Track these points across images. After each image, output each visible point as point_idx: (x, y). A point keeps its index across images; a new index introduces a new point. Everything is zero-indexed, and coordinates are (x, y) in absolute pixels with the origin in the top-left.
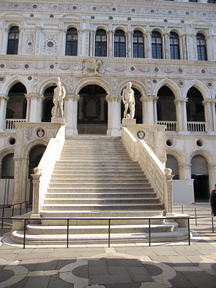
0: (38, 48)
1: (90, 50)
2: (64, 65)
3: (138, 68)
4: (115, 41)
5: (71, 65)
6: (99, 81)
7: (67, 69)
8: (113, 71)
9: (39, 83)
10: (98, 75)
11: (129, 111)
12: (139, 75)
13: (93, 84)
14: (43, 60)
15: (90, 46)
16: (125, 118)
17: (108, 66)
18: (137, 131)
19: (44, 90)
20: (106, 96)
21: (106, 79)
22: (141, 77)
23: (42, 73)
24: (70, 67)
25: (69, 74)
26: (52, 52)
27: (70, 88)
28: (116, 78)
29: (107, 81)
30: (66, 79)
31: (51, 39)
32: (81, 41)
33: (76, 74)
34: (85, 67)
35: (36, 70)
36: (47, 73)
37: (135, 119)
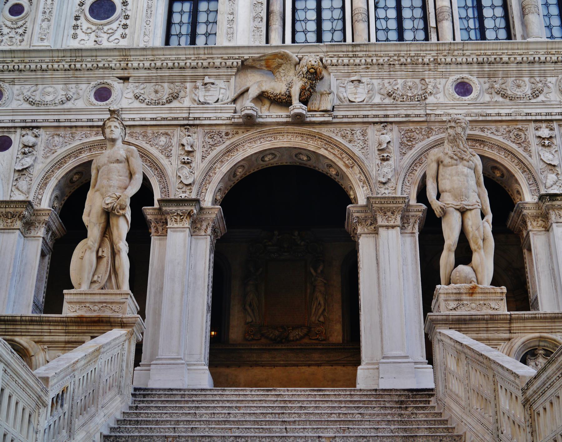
0: (49, 21)
1: (272, 22)
2: (158, 87)
3: (487, 86)
5: (188, 85)
6: (311, 145)
8: (377, 100)
9: (40, 159)
10: (308, 119)
11: (464, 254)
12: (496, 111)
13: (286, 161)
14: (67, 66)
15: (271, 8)
16: (449, 283)
17: (352, 81)
18: (516, 347)
19: (63, 193)
21: (344, 137)
22: (504, 118)
23: (58, 121)
24: (182, 94)
25: (176, 119)
26: (106, 36)
27: (180, 177)
28: (391, 130)
29: (350, 141)
30: (162, 143)
33: (209, 119)
34: (247, 90)
35: (34, 107)
36: (77, 120)
37: (504, 289)
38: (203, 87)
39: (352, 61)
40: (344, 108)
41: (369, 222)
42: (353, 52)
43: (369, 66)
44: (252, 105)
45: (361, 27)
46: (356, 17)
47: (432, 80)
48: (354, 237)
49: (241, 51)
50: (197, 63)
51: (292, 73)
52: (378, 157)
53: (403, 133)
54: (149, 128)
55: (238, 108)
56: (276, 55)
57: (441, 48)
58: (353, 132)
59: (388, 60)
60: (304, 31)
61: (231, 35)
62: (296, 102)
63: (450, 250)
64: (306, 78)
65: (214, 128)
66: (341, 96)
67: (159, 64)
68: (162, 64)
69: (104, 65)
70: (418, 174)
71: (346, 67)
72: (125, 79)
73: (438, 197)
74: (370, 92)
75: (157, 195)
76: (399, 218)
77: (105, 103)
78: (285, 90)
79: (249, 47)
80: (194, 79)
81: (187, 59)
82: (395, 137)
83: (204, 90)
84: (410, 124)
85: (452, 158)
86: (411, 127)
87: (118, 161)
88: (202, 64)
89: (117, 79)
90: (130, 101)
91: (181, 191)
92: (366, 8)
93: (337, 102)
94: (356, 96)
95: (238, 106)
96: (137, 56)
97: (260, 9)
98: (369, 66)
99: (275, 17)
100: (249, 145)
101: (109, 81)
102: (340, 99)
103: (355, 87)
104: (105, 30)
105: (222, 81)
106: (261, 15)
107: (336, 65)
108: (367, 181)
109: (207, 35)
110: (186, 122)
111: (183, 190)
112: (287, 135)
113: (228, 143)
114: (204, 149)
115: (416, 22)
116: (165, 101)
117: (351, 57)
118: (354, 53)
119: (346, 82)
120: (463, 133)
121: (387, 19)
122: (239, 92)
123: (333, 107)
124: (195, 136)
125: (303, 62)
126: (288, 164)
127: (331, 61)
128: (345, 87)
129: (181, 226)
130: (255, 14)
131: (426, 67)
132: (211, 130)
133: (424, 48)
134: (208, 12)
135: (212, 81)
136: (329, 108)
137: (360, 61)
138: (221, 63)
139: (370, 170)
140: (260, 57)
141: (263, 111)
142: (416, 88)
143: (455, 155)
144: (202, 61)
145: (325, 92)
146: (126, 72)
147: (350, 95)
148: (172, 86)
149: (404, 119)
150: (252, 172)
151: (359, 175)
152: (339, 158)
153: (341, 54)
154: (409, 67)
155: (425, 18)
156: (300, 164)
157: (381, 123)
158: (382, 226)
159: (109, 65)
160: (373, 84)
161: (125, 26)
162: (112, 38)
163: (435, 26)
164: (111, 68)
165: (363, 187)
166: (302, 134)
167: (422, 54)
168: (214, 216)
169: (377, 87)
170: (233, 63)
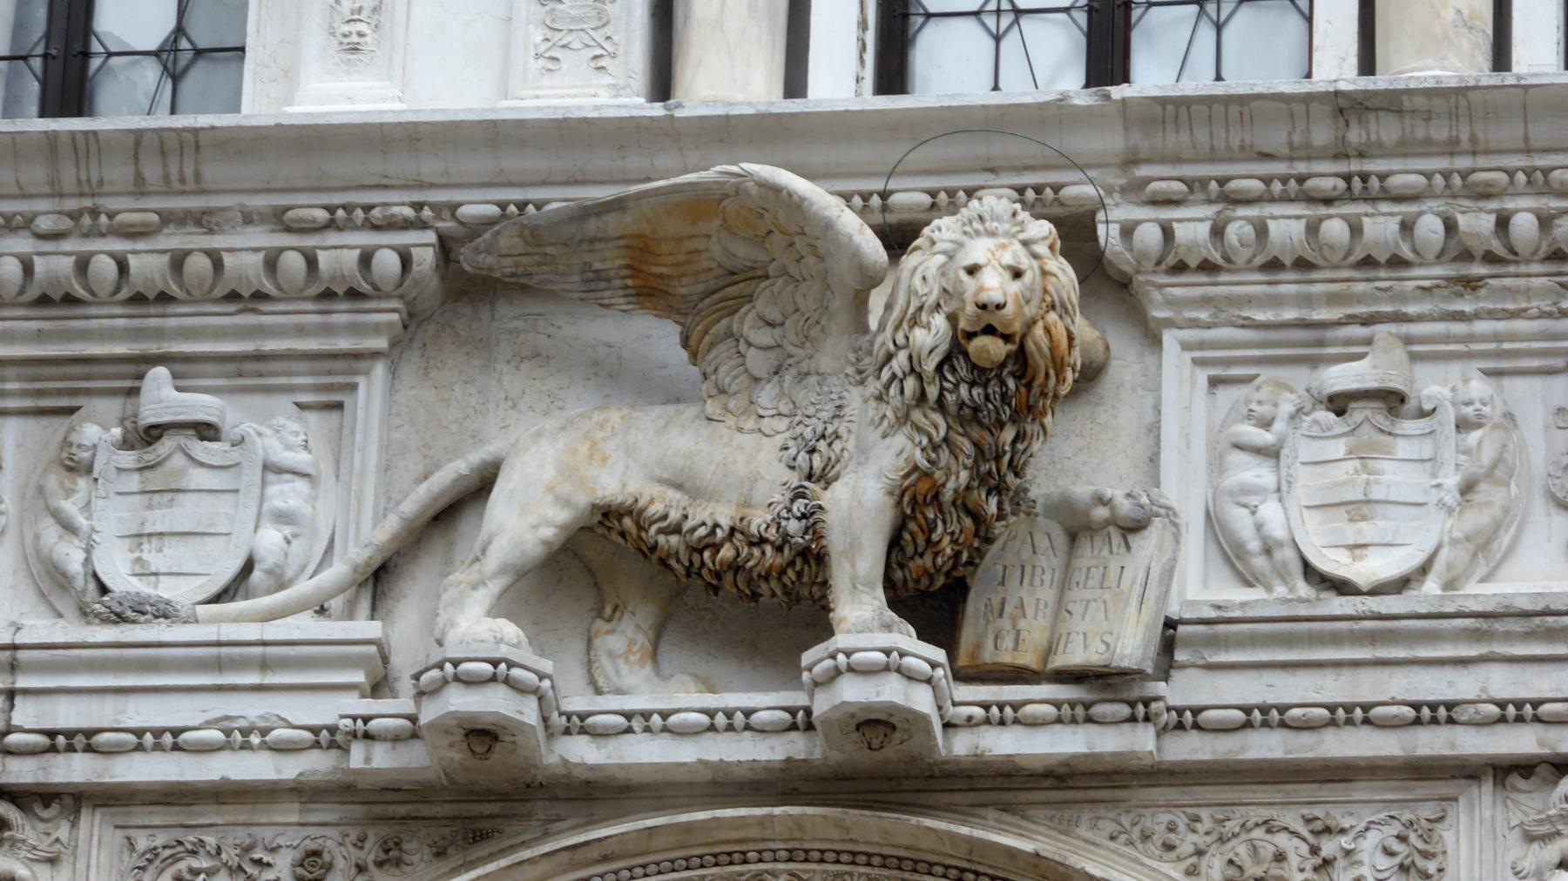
10: (961, 746)
17: (1339, 404)
33: (172, 740)
34: (479, 488)
38: (128, 458)
40: (1254, 641)
43: (1478, 270)
49: (429, 167)
50: (83, 264)
55: (403, 663)
58: (1329, 847)
64: (941, 405)
66: (1241, 522)
74: (1484, 490)
93: (1200, 587)
98: (1478, 270)
105: (285, 402)
107: (1207, 267)
117: (1328, 202)
118: (1355, 166)
119: (1287, 408)
122: (417, 499)
127: (1167, 232)
135: (202, 405)
137: (1407, 227)
138: (272, 263)
144: (119, 245)
145: (1101, 513)
147: (1313, 520)
170: (366, 259)
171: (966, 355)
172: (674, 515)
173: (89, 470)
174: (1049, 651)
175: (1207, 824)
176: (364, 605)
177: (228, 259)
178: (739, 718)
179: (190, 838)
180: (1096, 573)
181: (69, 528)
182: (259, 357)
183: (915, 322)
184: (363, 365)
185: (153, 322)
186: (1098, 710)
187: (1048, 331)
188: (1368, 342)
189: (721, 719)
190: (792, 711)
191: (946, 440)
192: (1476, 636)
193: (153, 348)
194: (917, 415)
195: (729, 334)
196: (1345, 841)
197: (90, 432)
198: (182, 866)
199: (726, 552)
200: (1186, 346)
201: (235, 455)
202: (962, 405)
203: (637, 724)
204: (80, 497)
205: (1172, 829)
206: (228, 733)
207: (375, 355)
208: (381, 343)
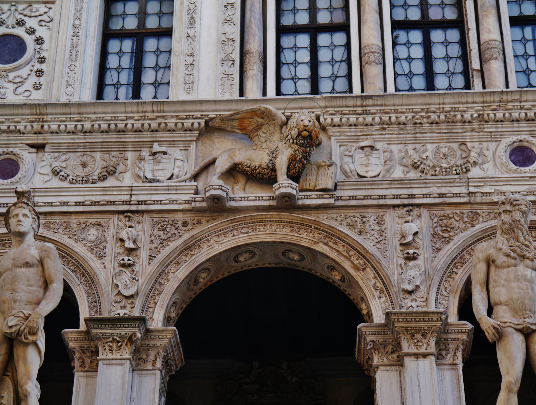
4: (400, 15)
5: (130, 155)
6: (305, 239)
7: (103, 178)
10: (300, 202)
15: (247, 47)
17: (362, 148)
20: (354, 330)
21: (351, 226)
25: (113, 203)
26: (11, 87)
27: (117, 286)
28: (419, 216)
29: (360, 233)
30: (92, 238)
31: (11, 21)
32: (192, 21)
33: (160, 202)
38: (151, 158)
39: (361, 119)
40: (351, 185)
41: (390, 348)
42: (362, 106)
43: (386, 126)
44: (221, 182)
45: (374, 71)
46: (367, 58)
47: (476, 144)
48: (368, 370)
49: (204, 107)
50: (143, 125)
51: (276, 137)
52: (400, 255)
53: (435, 220)
54: (73, 217)
56: (253, 113)
57: (488, 99)
58: (364, 220)
59: (413, 117)
60: (292, 79)
61: (190, 85)
62: (282, 179)
63: (510, 390)
64: (297, 144)
65: (166, 215)
66: (347, 168)
67: (88, 126)
68: (93, 126)
69: (9, 127)
70: (460, 278)
71: (353, 129)
72: (39, 147)
73: (490, 312)
74: (388, 162)
75: (84, 313)
76: (433, 343)
77: (9, 181)
78: (267, 161)
79: (215, 102)
80: (138, 147)
81: (128, 118)
82: (424, 226)
83: (152, 161)
84: (446, 208)
85: (508, 256)
86: (448, 211)
87: (27, 265)
88: (150, 125)
89: (28, 148)
90: (46, 178)
91: (118, 305)
92: (380, 44)
93: (340, 177)
94: (369, 169)
95: (201, 184)
96: (56, 114)
97: (231, 48)
98: (386, 126)
99: (252, 59)
100: (216, 239)
101: (16, 150)
102: (345, 173)
103: (367, 156)
104: (10, 79)
105: (178, 149)
106: (233, 56)
107: (339, 126)
108: (385, 288)
109: (157, 85)
110: (126, 208)
111: (122, 304)
112: (271, 225)
113: (186, 236)
114: (153, 246)
115: (452, 62)
116: (96, 177)
117: (360, 114)
118: (364, 108)
119: (353, 149)
120: (523, 220)
121: (409, 59)
122: (201, 164)
123: (336, 184)
124: (139, 227)
125: (292, 122)
126: (273, 265)
127: (332, 119)
128: (351, 156)
129: (118, 356)
130: (223, 56)
131: (468, 126)
132: (162, 218)
133: (464, 100)
134: (158, 52)
135: (163, 149)
136: (330, 185)
137: (373, 119)
138: (176, 124)
139: (389, 273)
140: (232, 115)
141: (236, 191)
142: (454, 156)
143: (513, 251)
144: (149, 122)
145: (323, 164)
146: (41, 137)
147: (359, 167)
148: (106, 156)
149: (437, 201)
150: (221, 277)
151: (373, 281)
152: (345, 257)
153: (346, 110)
154: (443, 126)
155: (465, 57)
156: (290, 264)
157: (405, 206)
158: (409, 355)
159: (16, 127)
160: (391, 151)
161: (40, 73)
162: (20, 90)
163: (479, 68)
164: (19, 131)
165: (380, 298)
166: (291, 224)
167: (461, 107)
168: (166, 341)
169: (397, 156)
170: (193, 124)
171: (301, 135)
172: (248, 165)
173: (144, 159)
174: (315, 187)
175: (343, 216)
176: (193, 180)
177: (168, 124)
178: (261, 198)
179: (163, 219)
180: (323, 174)
181: (140, 169)
182: (173, 141)
183: (292, 129)
184: (192, 142)
185: (155, 135)
186: (324, 196)
187: (315, 131)
188: (367, 139)
189: (257, 198)
190: (270, 197)
191: (298, 150)
192: (389, 184)
193: (155, 139)
194: (292, 145)
195: (257, 135)
196: (367, 219)
197: (144, 154)
198: (162, 224)
199: (258, 171)
200: (335, 140)
201: (170, 157)
202: (300, 143)
203: (243, 199)
204: (142, 164)
205: (337, 217)
206: (170, 201)
207: (194, 141)
208: (195, 139)
